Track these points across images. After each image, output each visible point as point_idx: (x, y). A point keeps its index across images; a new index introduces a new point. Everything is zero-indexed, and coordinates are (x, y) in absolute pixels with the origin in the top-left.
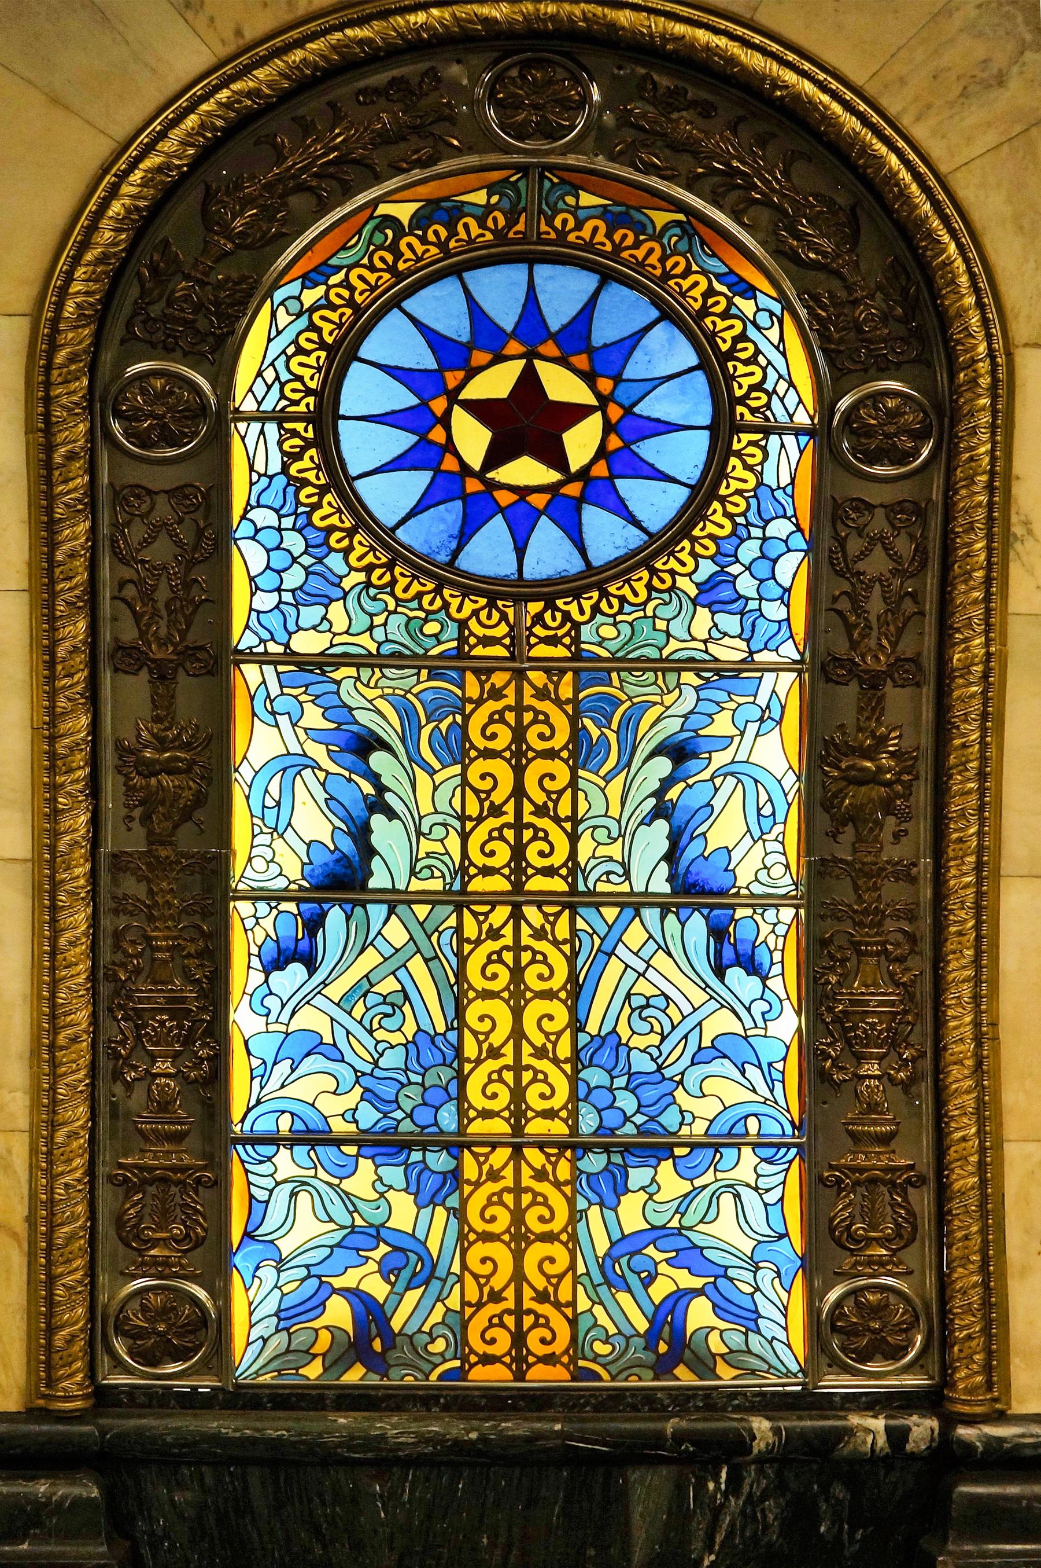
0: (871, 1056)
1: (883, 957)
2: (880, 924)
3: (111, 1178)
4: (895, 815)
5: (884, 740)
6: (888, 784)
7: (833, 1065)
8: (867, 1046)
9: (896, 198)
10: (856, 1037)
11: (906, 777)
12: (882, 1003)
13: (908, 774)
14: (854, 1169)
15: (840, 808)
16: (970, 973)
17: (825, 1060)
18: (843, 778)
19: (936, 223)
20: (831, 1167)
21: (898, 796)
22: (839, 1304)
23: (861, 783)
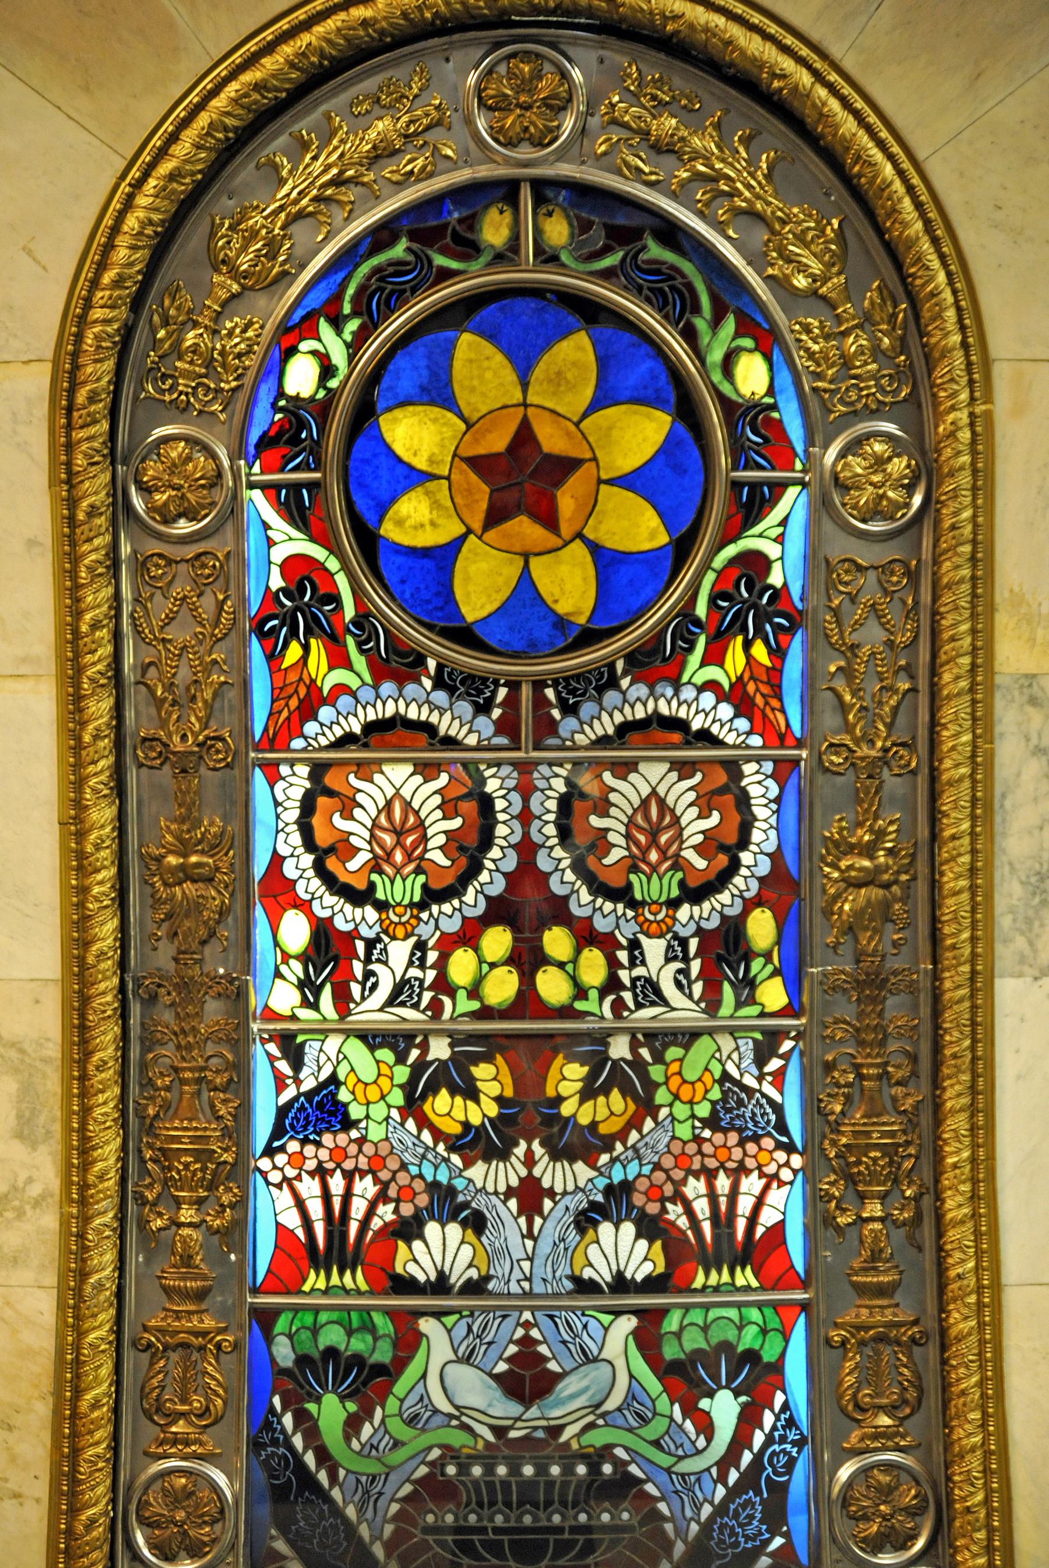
0: (873, 1196)
1: (885, 1081)
2: (882, 1043)
3: (134, 1344)
4: (893, 921)
5: (880, 835)
6: (887, 886)
7: (837, 1207)
8: (870, 1184)
9: (889, 215)
10: (859, 1173)
11: (904, 877)
12: (884, 1134)
13: (906, 873)
14: (859, 1328)
15: (840, 914)
16: (965, 1100)
17: (829, 1201)
18: (843, 880)
19: (926, 245)
20: (836, 1325)
21: (896, 900)
22: (850, 1484)
23: (859, 885)
